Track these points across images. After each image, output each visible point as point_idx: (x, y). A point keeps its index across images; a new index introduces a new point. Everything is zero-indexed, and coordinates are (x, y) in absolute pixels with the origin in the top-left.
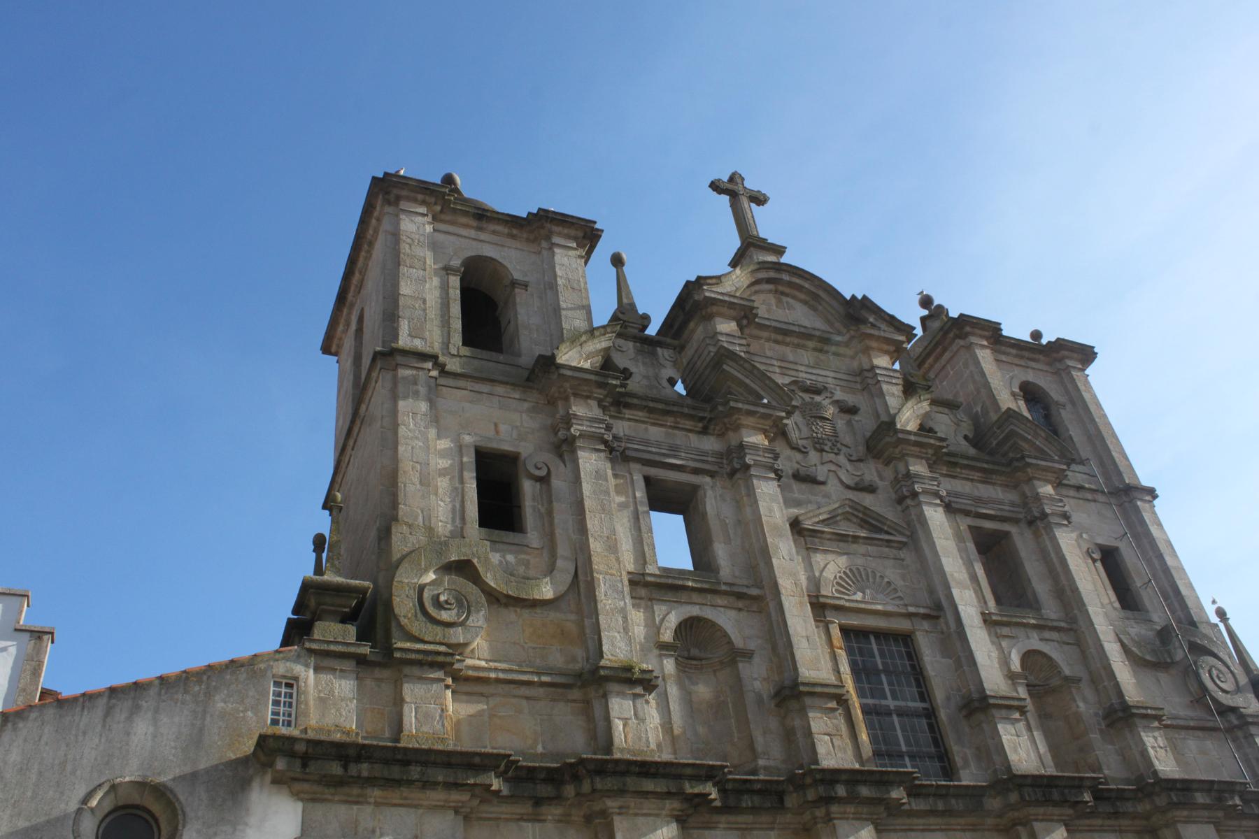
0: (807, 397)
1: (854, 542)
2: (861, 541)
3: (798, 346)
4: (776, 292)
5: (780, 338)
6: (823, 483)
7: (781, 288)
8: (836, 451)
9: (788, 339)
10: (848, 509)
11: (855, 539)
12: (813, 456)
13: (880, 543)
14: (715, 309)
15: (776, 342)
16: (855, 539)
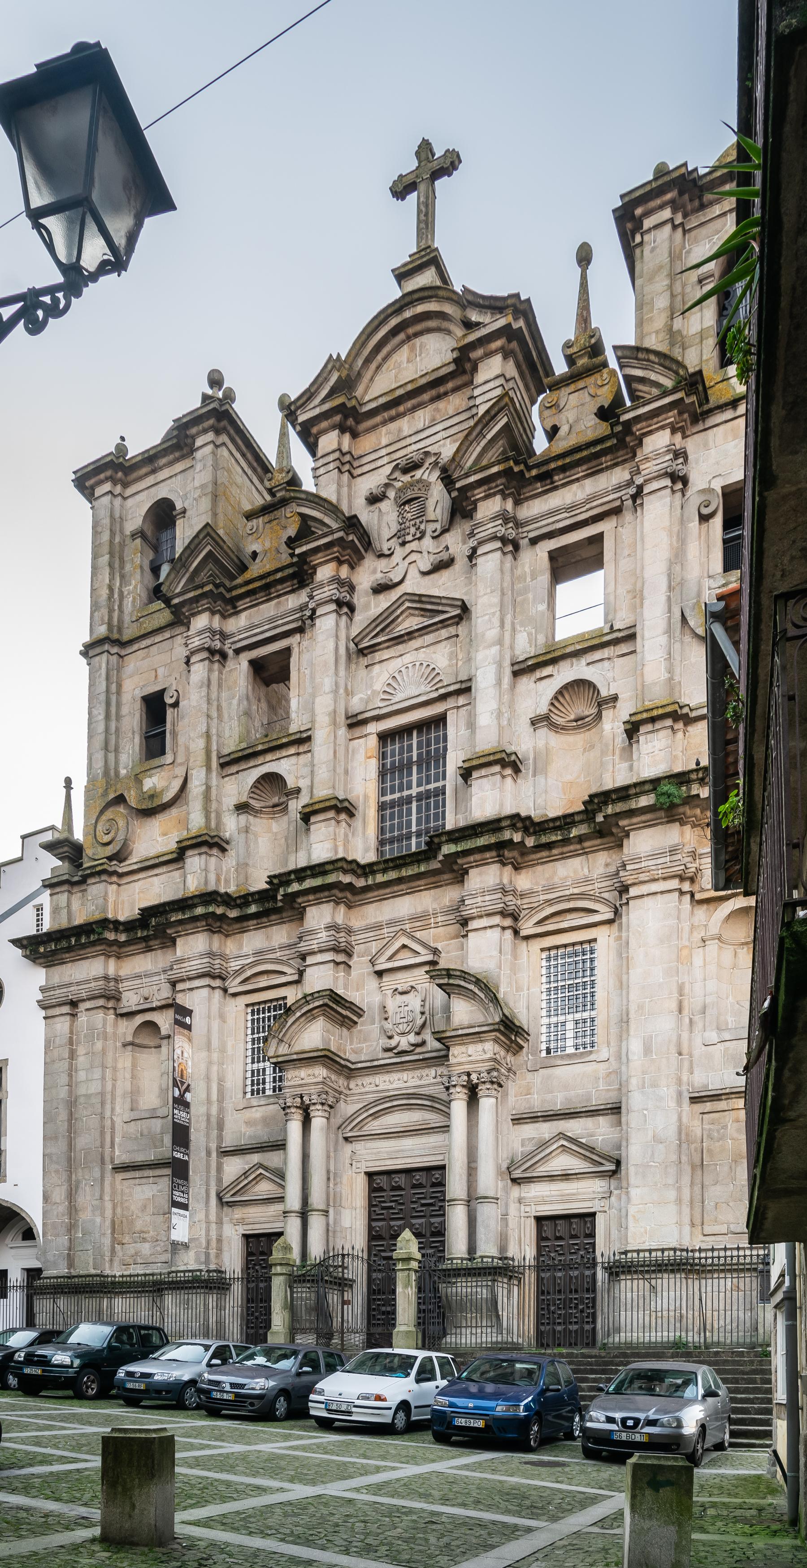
0: (406, 478)
1: (410, 639)
2: (416, 634)
3: (414, 409)
4: (409, 338)
5: (393, 412)
6: (402, 581)
7: (411, 331)
8: (418, 535)
9: (401, 409)
10: (407, 604)
11: (410, 635)
12: (399, 552)
13: (435, 627)
14: (314, 430)
15: (392, 419)
16: (410, 635)
